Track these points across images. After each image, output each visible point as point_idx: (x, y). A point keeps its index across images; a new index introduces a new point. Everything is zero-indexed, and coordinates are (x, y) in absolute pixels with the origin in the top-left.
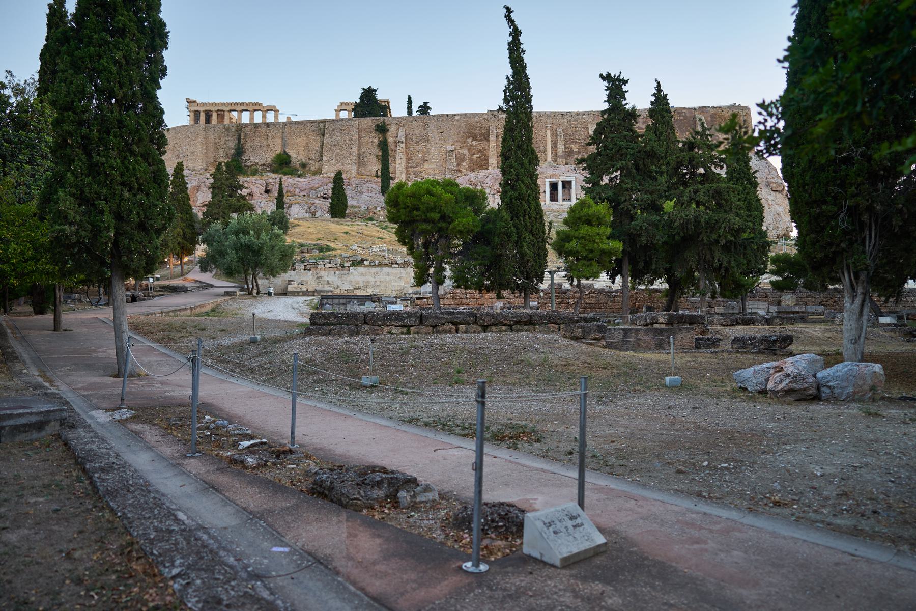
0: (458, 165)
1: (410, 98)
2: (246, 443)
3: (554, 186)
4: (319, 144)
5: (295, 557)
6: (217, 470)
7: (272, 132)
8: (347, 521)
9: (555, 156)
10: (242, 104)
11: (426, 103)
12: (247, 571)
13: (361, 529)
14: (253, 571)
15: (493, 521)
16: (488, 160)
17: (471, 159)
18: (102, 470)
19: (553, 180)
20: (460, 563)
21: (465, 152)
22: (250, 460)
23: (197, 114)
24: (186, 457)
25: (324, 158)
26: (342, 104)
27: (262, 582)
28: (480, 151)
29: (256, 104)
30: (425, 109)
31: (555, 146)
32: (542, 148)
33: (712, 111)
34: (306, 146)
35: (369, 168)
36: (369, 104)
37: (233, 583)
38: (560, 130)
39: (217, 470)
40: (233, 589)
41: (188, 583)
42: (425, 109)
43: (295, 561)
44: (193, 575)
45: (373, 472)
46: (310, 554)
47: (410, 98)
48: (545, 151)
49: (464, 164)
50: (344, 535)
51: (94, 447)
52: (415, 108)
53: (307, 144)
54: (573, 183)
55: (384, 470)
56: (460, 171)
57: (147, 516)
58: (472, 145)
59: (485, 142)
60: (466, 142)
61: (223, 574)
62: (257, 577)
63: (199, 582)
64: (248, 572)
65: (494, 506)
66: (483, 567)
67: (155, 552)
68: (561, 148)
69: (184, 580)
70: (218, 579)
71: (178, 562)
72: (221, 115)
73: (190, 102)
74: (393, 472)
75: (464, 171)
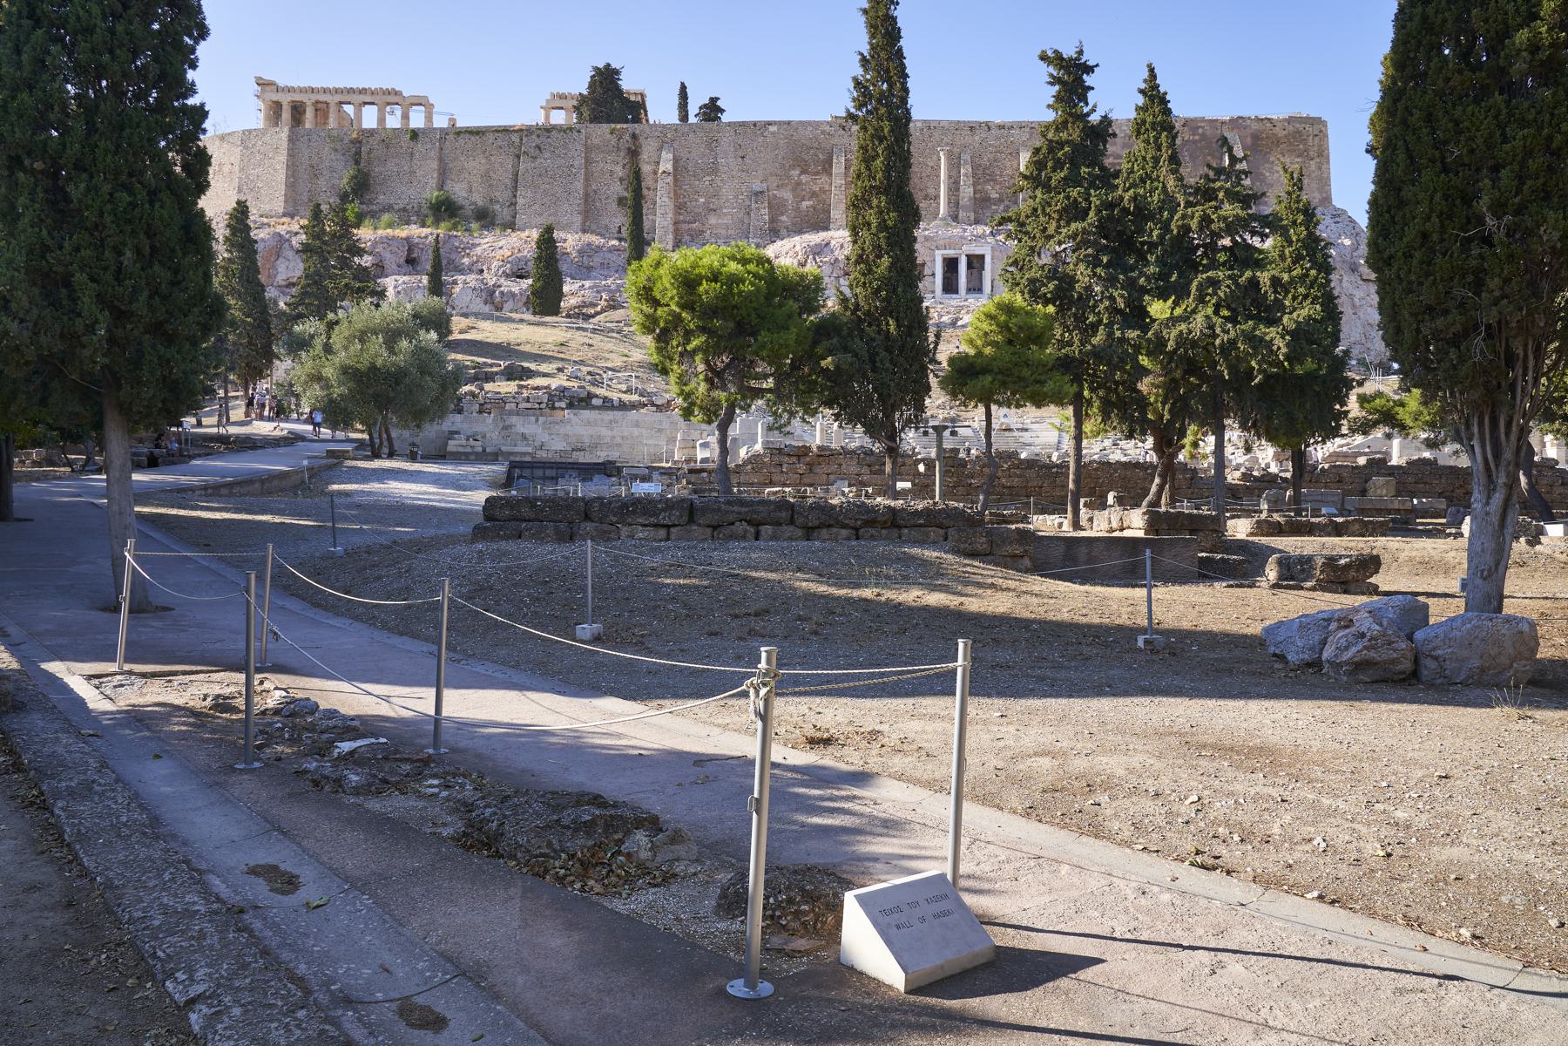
0: (773, 220)
1: (683, 88)
2: (346, 746)
3: (951, 265)
5: (420, 966)
6: (291, 795)
8: (523, 897)
9: (954, 203)
10: (363, 91)
11: (714, 100)
12: (329, 990)
13: (547, 913)
14: (341, 991)
15: (790, 901)
18: (71, 792)
19: (951, 253)
20: (720, 981)
21: (786, 194)
22: (354, 778)
23: (277, 106)
24: (232, 770)
25: (520, 201)
27: (355, 1011)
28: (814, 194)
29: (389, 92)
30: (712, 110)
31: (954, 188)
32: (931, 191)
33: (1255, 126)
34: (486, 176)
35: (605, 221)
36: (608, 99)
37: (301, 1014)
38: (966, 157)
39: (291, 795)
40: (298, 1026)
41: (216, 1013)
43: (422, 972)
44: (227, 999)
45: (578, 804)
46: (449, 960)
47: (683, 88)
48: (937, 197)
49: (784, 218)
50: (515, 924)
51: (60, 750)
53: (487, 171)
54: (988, 259)
55: (597, 800)
57: (151, 884)
58: (799, 184)
59: (825, 178)
60: (789, 177)
61: (283, 998)
62: (348, 1001)
63: (237, 1011)
64: (332, 993)
65: (795, 872)
66: (766, 988)
67: (160, 954)
69: (210, 1006)
70: (271, 1006)
71: (200, 974)
72: (321, 110)
73: (263, 84)
74: (615, 805)
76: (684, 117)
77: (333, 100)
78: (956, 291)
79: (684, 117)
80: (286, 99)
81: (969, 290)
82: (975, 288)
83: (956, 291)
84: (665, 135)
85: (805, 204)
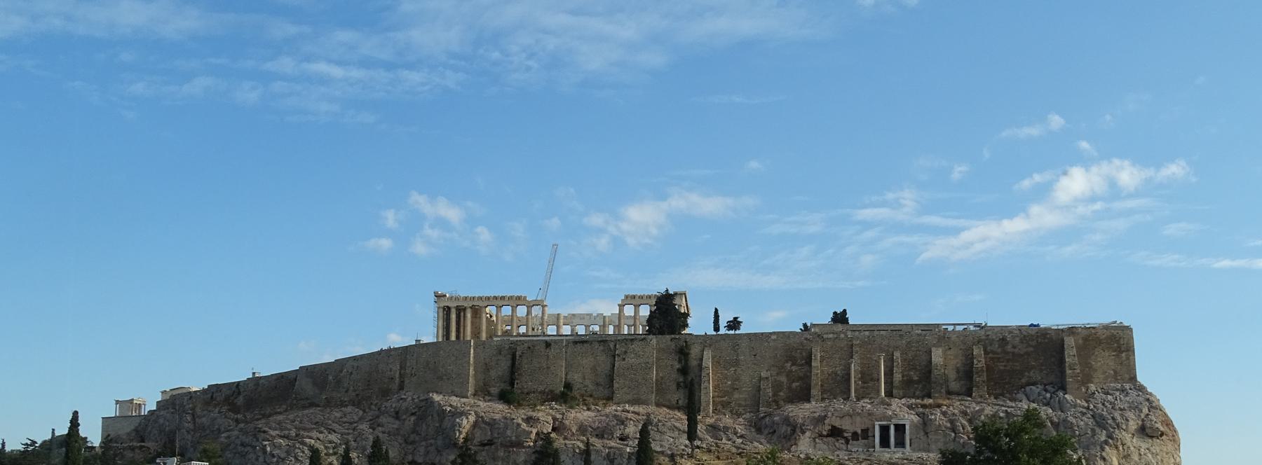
1: (716, 310)
3: (884, 430)
4: (609, 366)
7: (553, 352)
9: (889, 383)
10: (503, 298)
16: (809, 390)
17: (789, 388)
21: (783, 379)
23: (447, 310)
25: (616, 385)
26: (627, 297)
28: (800, 378)
29: (519, 298)
31: (889, 373)
33: (1085, 332)
34: (594, 369)
36: (667, 313)
38: (897, 354)
42: (734, 324)
47: (716, 310)
48: (878, 380)
52: (723, 323)
54: (907, 427)
56: (776, 402)
59: (806, 368)
60: (783, 367)
68: (898, 377)
72: (477, 312)
75: (782, 403)
76: (717, 328)
77: (481, 304)
78: (888, 446)
79: (717, 328)
80: (453, 305)
81: (897, 445)
82: (900, 443)
83: (888, 446)
84: (705, 340)
85: (794, 385)
